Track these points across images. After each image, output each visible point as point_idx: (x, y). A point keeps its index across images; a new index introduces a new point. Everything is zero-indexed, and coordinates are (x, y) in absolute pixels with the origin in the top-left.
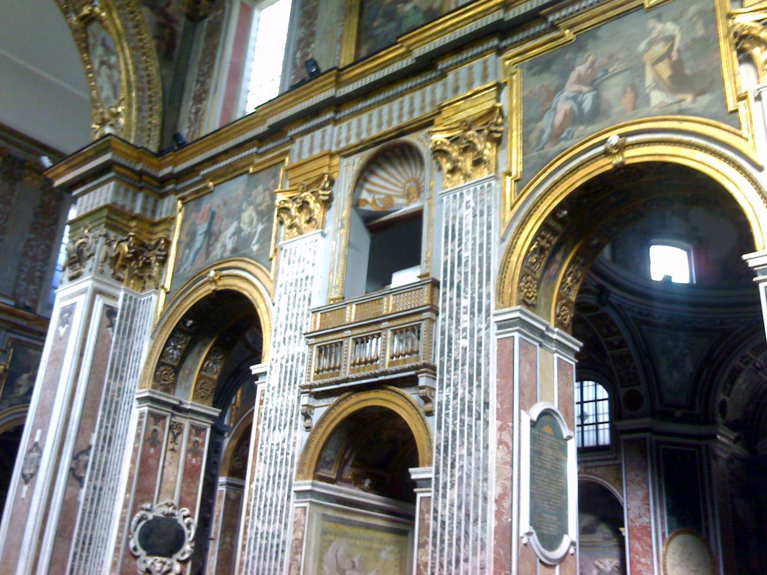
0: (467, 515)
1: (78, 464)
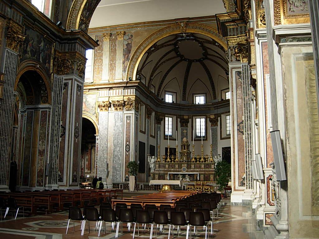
1: (240, 128)
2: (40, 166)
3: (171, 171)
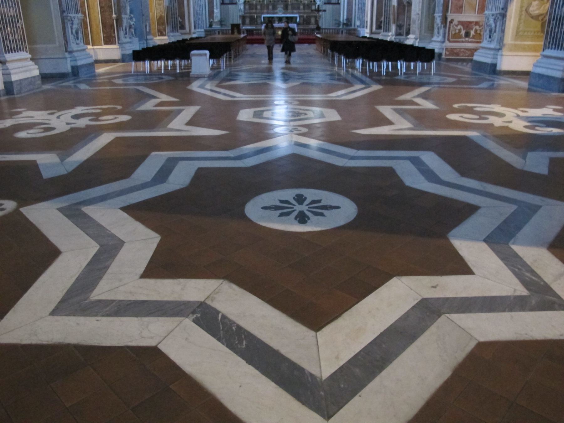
2: (159, 11)
3: (263, 13)
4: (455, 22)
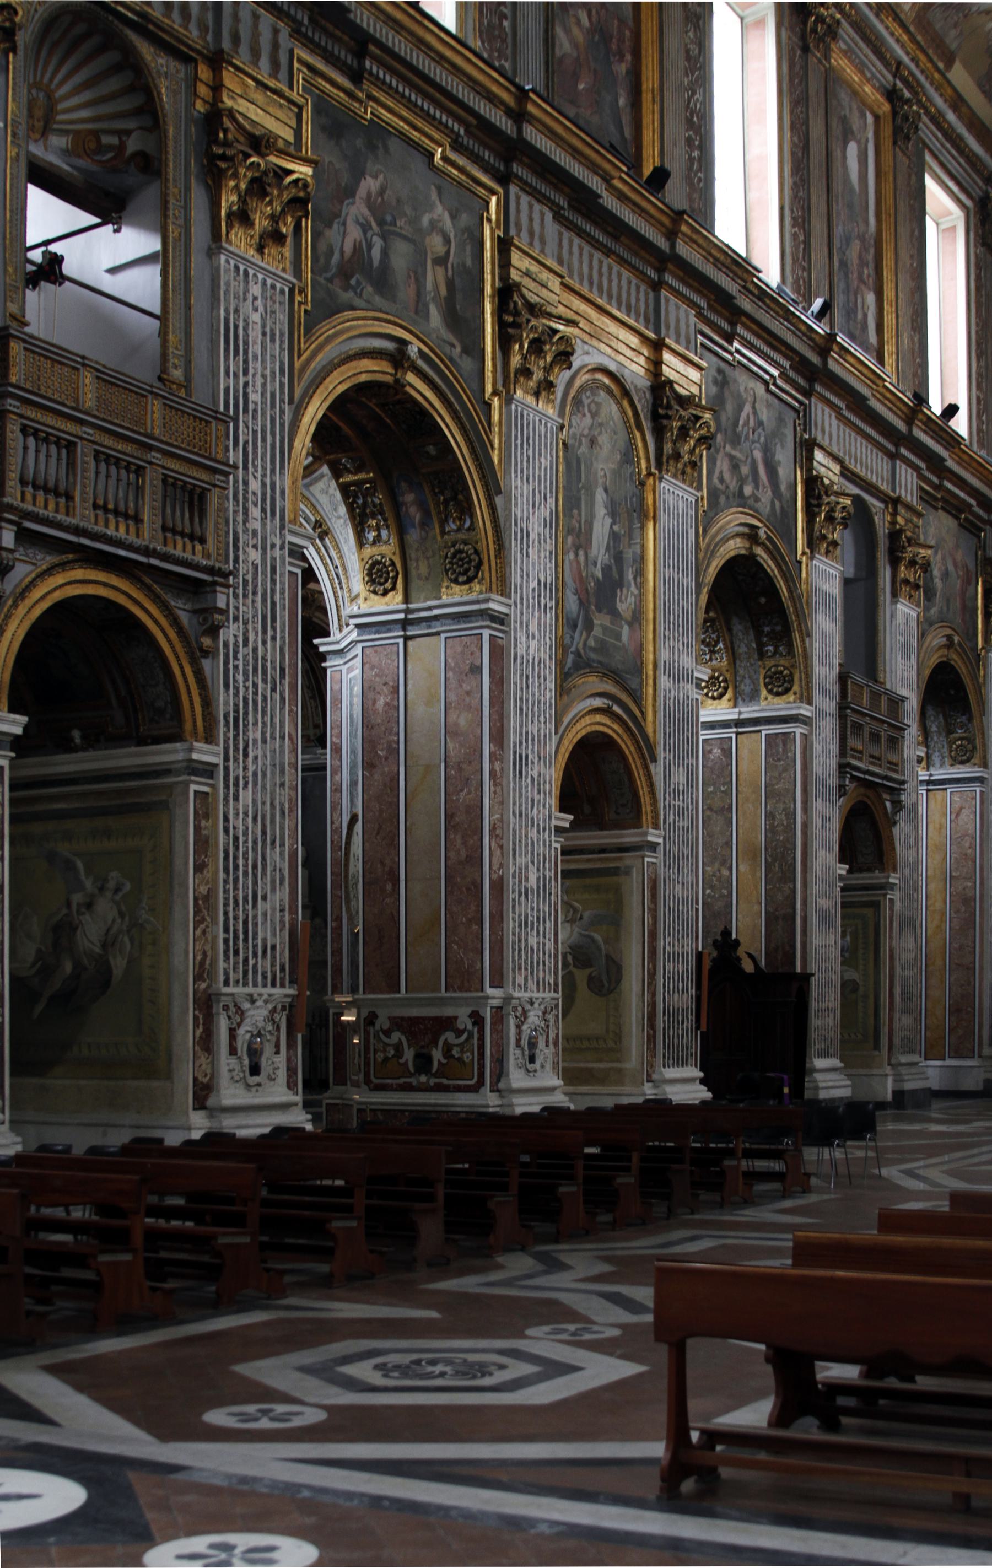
0: (264, 833)
4: (382, 1022)
